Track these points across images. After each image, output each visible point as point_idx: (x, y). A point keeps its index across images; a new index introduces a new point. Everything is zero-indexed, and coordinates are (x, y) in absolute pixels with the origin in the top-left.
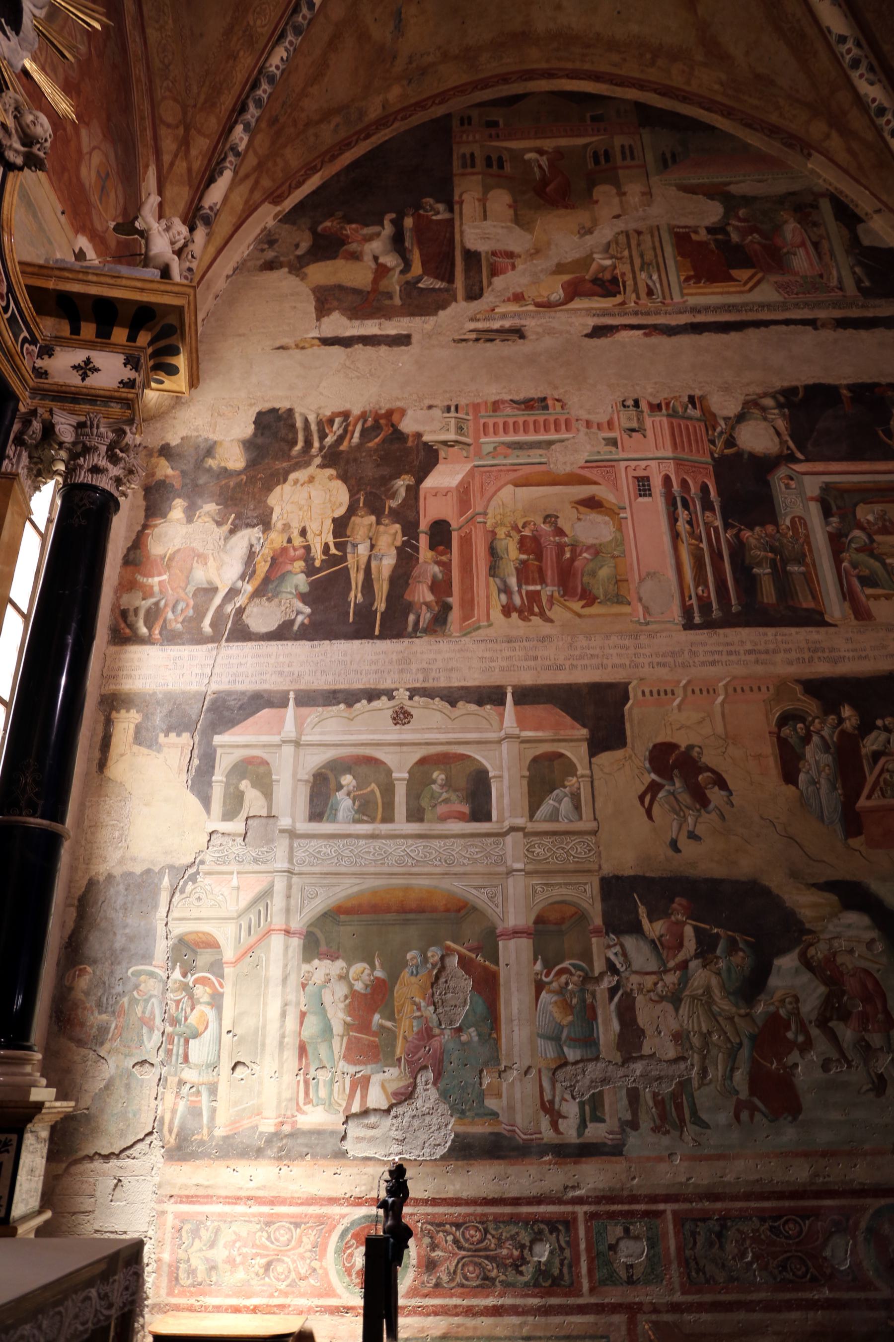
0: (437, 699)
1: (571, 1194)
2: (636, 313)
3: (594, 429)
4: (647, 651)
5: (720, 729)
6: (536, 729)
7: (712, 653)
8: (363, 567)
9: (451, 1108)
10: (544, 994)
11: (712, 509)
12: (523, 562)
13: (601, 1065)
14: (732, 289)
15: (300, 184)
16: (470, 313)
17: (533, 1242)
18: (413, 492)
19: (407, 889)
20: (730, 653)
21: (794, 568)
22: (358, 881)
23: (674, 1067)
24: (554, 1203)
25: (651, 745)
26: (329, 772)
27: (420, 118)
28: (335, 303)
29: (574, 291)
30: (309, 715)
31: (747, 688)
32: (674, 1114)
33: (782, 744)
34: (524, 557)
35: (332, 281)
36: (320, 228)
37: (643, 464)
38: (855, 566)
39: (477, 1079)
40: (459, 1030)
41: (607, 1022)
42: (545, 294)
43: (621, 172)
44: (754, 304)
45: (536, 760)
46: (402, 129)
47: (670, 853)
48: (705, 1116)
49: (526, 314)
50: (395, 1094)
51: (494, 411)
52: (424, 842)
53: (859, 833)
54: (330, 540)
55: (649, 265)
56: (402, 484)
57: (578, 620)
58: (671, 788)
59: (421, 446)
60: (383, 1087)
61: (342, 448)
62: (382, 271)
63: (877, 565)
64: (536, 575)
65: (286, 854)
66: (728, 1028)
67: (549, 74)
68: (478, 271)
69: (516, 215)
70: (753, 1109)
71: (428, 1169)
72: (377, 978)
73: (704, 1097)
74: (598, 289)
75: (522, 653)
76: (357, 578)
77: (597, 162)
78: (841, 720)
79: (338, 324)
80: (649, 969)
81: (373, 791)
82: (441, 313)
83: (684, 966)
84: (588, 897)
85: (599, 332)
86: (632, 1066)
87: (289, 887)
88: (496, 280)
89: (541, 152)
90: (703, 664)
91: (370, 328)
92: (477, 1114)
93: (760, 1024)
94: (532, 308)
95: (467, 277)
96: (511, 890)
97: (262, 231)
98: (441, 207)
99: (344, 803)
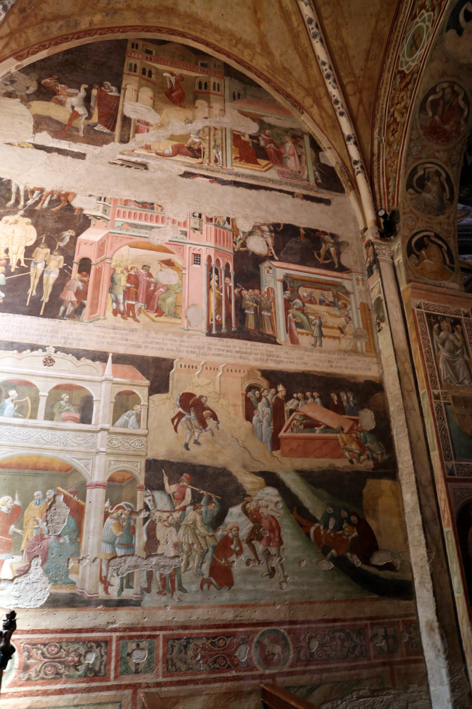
1: (111, 626)
2: (207, 170)
3: (176, 225)
4: (186, 344)
5: (217, 389)
7: (219, 350)
8: (39, 276)
9: (50, 579)
10: (108, 519)
11: (230, 277)
12: (128, 288)
13: (134, 558)
16: (121, 150)
17: (86, 653)
18: (74, 240)
19: (39, 457)
20: (228, 351)
21: (265, 313)
22: (11, 450)
23: (173, 560)
24: (100, 631)
25: (181, 393)
27: (110, 36)
28: (46, 127)
29: (178, 151)
31: (233, 370)
32: (170, 585)
33: (247, 400)
34: (129, 285)
35: (46, 113)
37: (199, 247)
38: (294, 317)
39: (66, 564)
40: (59, 536)
41: (140, 536)
42: (162, 149)
43: (212, 96)
44: (266, 178)
45: (119, 394)
46: (99, 40)
47: (184, 450)
48: (185, 586)
49: (150, 157)
50: (18, 571)
51: (125, 205)
52: (52, 432)
53: (278, 449)
54: (22, 258)
55: (218, 146)
56: (68, 234)
57: (152, 323)
58: (189, 417)
59: (82, 216)
60: (11, 567)
61: (37, 208)
62: (75, 115)
63: (304, 318)
64: (134, 296)
66: (202, 542)
67: (183, 35)
68: (129, 129)
69: (154, 103)
70: (210, 583)
71: (31, 613)
72: (15, 505)
73: (186, 577)
74: (190, 153)
75: (120, 336)
76: (34, 282)
77: (200, 87)
78: (277, 392)
79: (44, 138)
80: (166, 510)
81: (26, 401)
82: (105, 146)
83: (184, 509)
84: (139, 470)
85: (187, 175)
86: (151, 559)
88: (137, 135)
89: (172, 74)
90: (214, 355)
91: (63, 145)
92: (64, 583)
93: (219, 540)
94: (154, 154)
95: (122, 130)
96: (97, 462)
98: (114, 88)
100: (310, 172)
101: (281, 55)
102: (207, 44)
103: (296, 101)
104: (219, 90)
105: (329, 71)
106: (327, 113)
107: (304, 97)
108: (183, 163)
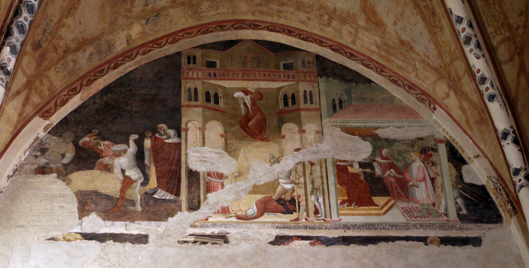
2: (306, 227)
14: (374, 212)
15: (64, 103)
16: (191, 221)
27: (157, 54)
28: (93, 206)
29: (264, 208)
35: (91, 187)
36: (81, 142)
42: (244, 209)
43: (302, 113)
44: (386, 223)
46: (144, 62)
49: (230, 224)
55: (317, 190)
62: (127, 182)
67: (255, 26)
68: (199, 186)
69: (226, 143)
74: (281, 207)
77: (286, 104)
79: (95, 223)
82: (170, 219)
85: (280, 240)
88: (209, 195)
89: (246, 92)
91: (119, 227)
94: (234, 219)
95: (189, 192)
97: (36, 140)
98: (171, 132)
100: (450, 201)
101: (395, 23)
102: (289, 31)
103: (423, 93)
104: (312, 103)
105: (468, 30)
106: (471, 101)
107: (435, 83)
108: (273, 223)
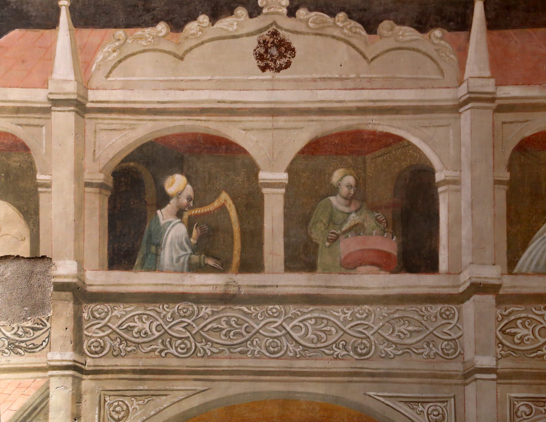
0: (341, 15)
6: (527, 82)
22: (200, 386)
26: (141, 168)
30: (99, 47)
45: (524, 147)
52: (312, 312)
65: (69, 333)
81: (223, 208)
87: (77, 398)
96: (471, 409)
99: (174, 233)
